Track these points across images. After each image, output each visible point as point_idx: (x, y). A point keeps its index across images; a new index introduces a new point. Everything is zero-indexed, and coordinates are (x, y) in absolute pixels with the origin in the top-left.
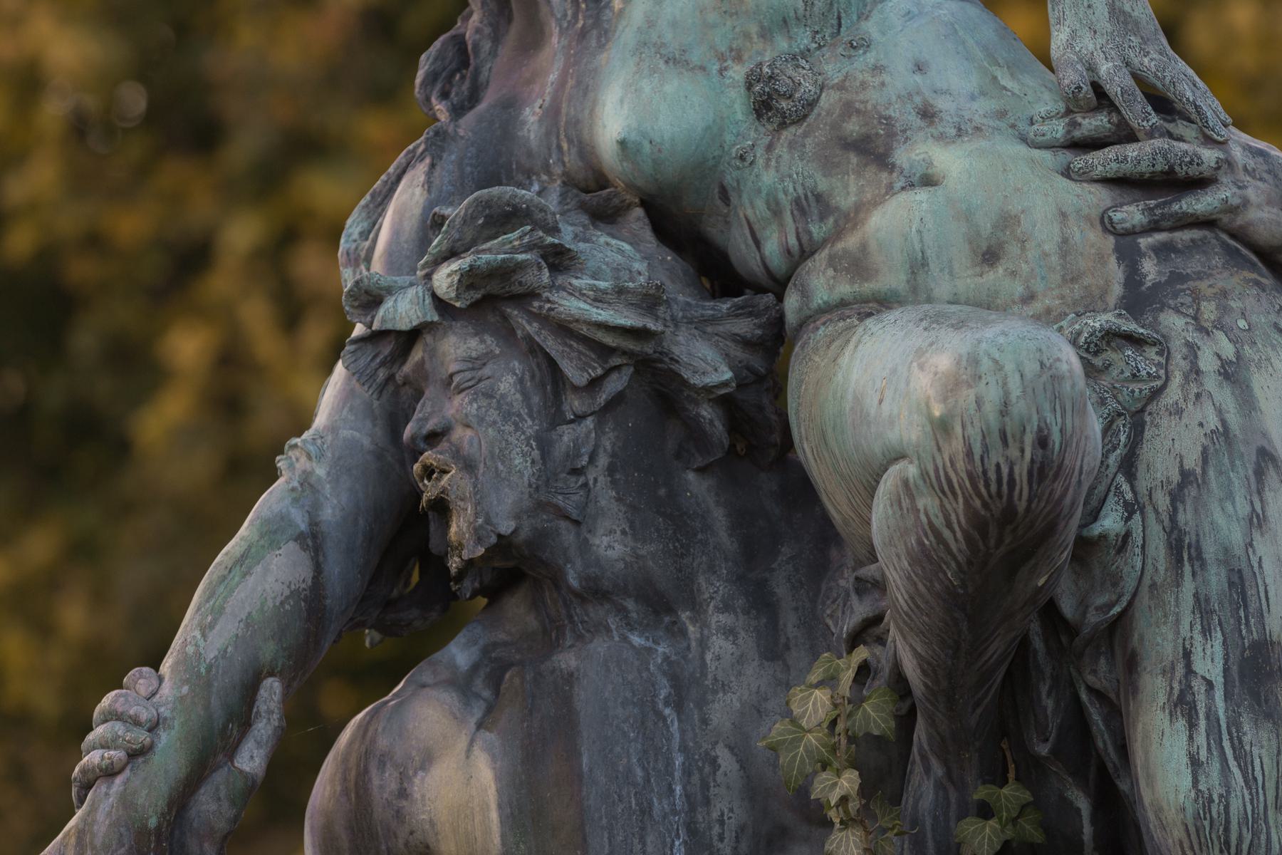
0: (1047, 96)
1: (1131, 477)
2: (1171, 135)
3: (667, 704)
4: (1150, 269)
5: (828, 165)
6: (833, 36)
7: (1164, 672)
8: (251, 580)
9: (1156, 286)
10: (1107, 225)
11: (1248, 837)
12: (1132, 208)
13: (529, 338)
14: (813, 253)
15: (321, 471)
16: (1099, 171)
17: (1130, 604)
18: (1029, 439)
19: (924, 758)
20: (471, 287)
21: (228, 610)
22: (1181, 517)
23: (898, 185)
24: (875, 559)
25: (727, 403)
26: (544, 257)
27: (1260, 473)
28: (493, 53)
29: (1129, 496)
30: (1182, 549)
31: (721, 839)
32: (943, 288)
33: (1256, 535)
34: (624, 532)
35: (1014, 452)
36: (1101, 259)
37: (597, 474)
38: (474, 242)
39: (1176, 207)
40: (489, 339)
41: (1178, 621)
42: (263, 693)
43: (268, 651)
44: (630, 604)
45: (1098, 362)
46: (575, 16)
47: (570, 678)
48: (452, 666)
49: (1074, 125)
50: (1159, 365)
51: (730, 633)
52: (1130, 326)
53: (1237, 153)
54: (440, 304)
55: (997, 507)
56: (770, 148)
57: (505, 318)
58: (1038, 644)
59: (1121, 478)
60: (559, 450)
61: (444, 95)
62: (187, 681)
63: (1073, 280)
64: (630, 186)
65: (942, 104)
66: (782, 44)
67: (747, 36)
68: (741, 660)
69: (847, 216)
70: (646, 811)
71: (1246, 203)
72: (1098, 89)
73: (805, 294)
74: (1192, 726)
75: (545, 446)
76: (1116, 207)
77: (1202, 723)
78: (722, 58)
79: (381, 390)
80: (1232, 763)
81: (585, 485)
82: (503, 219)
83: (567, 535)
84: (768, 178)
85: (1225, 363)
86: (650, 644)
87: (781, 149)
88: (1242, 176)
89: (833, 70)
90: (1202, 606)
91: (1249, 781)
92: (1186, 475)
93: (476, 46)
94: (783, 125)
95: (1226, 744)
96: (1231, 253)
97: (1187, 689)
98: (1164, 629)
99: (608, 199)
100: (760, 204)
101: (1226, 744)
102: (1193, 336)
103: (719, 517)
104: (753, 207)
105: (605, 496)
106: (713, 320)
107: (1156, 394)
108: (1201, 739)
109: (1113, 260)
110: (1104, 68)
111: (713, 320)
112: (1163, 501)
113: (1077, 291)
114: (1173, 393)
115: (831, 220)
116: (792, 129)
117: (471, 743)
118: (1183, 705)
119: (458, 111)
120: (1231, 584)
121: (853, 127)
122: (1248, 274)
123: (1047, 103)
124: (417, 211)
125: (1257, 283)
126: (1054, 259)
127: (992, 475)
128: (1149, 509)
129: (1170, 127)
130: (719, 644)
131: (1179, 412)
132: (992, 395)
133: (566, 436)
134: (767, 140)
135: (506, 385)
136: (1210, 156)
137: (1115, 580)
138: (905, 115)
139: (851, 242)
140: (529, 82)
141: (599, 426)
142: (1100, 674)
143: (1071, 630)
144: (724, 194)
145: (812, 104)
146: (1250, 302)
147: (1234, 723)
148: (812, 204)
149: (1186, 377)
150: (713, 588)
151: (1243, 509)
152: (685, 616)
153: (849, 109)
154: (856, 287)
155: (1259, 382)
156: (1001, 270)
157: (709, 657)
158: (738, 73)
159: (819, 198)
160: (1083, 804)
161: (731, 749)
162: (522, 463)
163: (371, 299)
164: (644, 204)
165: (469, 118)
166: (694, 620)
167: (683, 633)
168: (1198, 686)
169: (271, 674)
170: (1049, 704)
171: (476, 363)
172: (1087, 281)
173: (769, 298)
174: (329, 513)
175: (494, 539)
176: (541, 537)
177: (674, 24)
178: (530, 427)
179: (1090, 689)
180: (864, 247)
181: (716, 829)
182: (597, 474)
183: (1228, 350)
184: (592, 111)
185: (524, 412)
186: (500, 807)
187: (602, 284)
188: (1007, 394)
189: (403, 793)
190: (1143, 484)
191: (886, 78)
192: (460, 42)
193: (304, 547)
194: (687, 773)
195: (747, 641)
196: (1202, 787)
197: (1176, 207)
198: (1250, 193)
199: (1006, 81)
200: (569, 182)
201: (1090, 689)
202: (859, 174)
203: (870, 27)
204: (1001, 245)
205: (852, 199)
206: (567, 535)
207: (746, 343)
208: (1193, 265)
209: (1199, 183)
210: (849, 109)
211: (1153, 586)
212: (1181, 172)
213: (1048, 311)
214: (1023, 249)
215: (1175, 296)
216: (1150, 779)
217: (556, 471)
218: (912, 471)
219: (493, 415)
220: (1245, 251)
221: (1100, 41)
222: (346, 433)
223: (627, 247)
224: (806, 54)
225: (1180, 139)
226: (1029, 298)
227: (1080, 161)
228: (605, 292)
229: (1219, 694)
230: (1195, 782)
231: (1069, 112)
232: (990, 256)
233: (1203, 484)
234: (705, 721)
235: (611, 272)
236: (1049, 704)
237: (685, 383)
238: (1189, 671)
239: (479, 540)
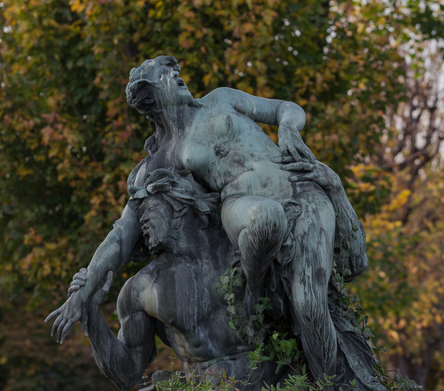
0: (277, 152)
2: (303, 161)
3: (194, 278)
4: (298, 189)
6: (233, 138)
7: (299, 274)
8: (107, 250)
9: (300, 193)
10: (290, 180)
11: (316, 310)
12: (295, 176)
13: (167, 201)
14: (227, 184)
15: (122, 227)
16: (288, 168)
17: (292, 260)
18: (272, 225)
19: (248, 291)
20: (155, 189)
21: (102, 256)
22: (304, 242)
23: (246, 170)
24: (239, 249)
25: (208, 215)
26: (171, 184)
27: (320, 233)
28: (161, 140)
29: (293, 237)
30: (303, 248)
31: (205, 307)
32: (254, 192)
33: (319, 246)
34: (186, 242)
35: (269, 227)
36: (288, 187)
37: (181, 230)
38: (156, 180)
39: (304, 176)
40: (158, 200)
41: (302, 264)
42: (109, 274)
43: (110, 265)
44: (187, 257)
45: (287, 208)
46: (178, 133)
47: (174, 272)
48: (149, 270)
49: (283, 158)
50: (300, 210)
51: (208, 264)
52: (294, 201)
53: (317, 165)
54: (148, 193)
55: (265, 239)
56: (219, 162)
57: (162, 196)
58: (273, 268)
59: (291, 233)
60: (173, 224)
61: (150, 149)
62: (93, 271)
63: (282, 191)
64: (189, 169)
65: (255, 153)
66: (222, 140)
67: (215, 138)
68: (210, 270)
69: (235, 177)
70: (189, 301)
71: (319, 176)
72: (288, 151)
73: (225, 193)
74: (305, 286)
75: (170, 223)
76: (292, 176)
77: (307, 285)
78: (209, 143)
79: (135, 211)
80: (313, 294)
81: (178, 232)
82: (163, 175)
83: (174, 242)
84: (218, 168)
85: (313, 210)
86: (191, 266)
87: (221, 162)
88: (318, 170)
89: (232, 145)
90: (308, 261)
91: (317, 298)
92: (305, 233)
93: (157, 139)
94: (222, 157)
95: (312, 290)
96: (315, 186)
98: (299, 265)
99: (184, 172)
100: (216, 174)
101: (312, 290)
102: (307, 204)
103: (206, 239)
104: (215, 174)
105: (182, 234)
106: (206, 198)
107: (299, 216)
108: (307, 289)
109: (291, 187)
110: (290, 147)
111: (206, 198)
112: (300, 238)
113: (283, 194)
114: (303, 216)
115: (231, 177)
116: (224, 158)
117: (153, 286)
118: (303, 281)
119: (153, 152)
120: (314, 256)
121: (236, 158)
122: (319, 191)
123: (278, 154)
124: (144, 173)
125: (321, 193)
126: (278, 187)
127: (264, 232)
128: (297, 240)
129: (303, 159)
130: (205, 266)
131: (304, 220)
132: (264, 215)
133: (174, 221)
134: (218, 160)
135: (162, 210)
136: (311, 166)
137: (289, 255)
138: (247, 156)
139: (235, 182)
140: (168, 147)
141: (181, 220)
142: (286, 274)
143: (280, 265)
144: (209, 171)
145: (228, 153)
146: (319, 197)
147: (314, 286)
148: (227, 174)
149: (305, 212)
150: (205, 254)
152: (198, 260)
153: (236, 154)
154: (236, 192)
155: (321, 214)
156: (267, 189)
157: (203, 269)
158: (213, 146)
159: (229, 172)
160: (281, 302)
161: (207, 288)
162: (165, 227)
163: (134, 191)
164: (192, 173)
165: (155, 154)
166: (200, 261)
167: (198, 264)
168: (306, 277)
169: (111, 270)
170: (275, 280)
171: (156, 205)
172: (285, 191)
173: (218, 193)
174: (124, 236)
175: (158, 243)
176: (168, 242)
177: (199, 135)
178: (167, 219)
179: (284, 278)
180: (238, 183)
181: (204, 305)
182: (181, 230)
183: (314, 207)
184: (181, 153)
185: (166, 216)
186: (158, 299)
187: (183, 190)
188: (267, 215)
189: (138, 296)
190: (296, 234)
191: (243, 147)
192: (154, 138)
193: (118, 244)
194: (198, 293)
195: (211, 266)
196: (307, 299)
197: (304, 176)
198: (320, 174)
199: (269, 149)
200: (176, 168)
201: (284, 278)
202: (237, 168)
203: (241, 137)
204: (267, 183)
205: (236, 173)
206: (174, 242)
207: (213, 203)
208: (308, 188)
209: (309, 171)
210: (236, 154)
211: (297, 256)
212: (305, 169)
213: (277, 198)
214: (272, 184)
215: (304, 195)
216: (296, 298)
217: (172, 229)
219: (159, 217)
220: (318, 186)
221: (289, 141)
222: (128, 220)
223: (188, 182)
224: (227, 142)
225: (305, 162)
226: (273, 195)
227: (284, 166)
228: (183, 191)
229: (311, 279)
230: (305, 298)
231: (282, 156)
232: (265, 186)
233: (308, 235)
234: (202, 282)
235: (184, 187)
236: (275, 280)
237: (199, 211)
238: (305, 274)
239: (155, 243)
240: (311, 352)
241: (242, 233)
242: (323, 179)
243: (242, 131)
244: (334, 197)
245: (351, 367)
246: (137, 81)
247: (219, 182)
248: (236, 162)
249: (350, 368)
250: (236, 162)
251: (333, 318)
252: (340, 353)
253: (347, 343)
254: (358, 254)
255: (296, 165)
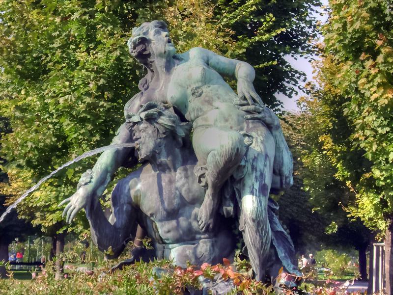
1: (246, 157)
5: (203, 104)
18: (236, 149)
19: (208, 195)
25: (183, 139)
27: (266, 158)
28: (151, 82)
30: (254, 168)
37: (163, 147)
43: (109, 169)
54: (141, 119)
56: (194, 100)
58: (229, 181)
67: (192, 83)
68: (181, 178)
73: (197, 123)
78: (187, 86)
91: (261, 206)
92: (255, 157)
97: (253, 190)
102: (257, 136)
112: (251, 161)
121: (207, 99)
135: (150, 132)
136: (261, 109)
137: (243, 172)
139: (205, 116)
151: (264, 163)
153: (206, 96)
159: (201, 109)
168: (255, 190)
171: (146, 128)
179: (237, 189)
182: (163, 147)
201: (237, 189)
207: (187, 129)
218: (216, 152)
226: (231, 128)
227: (241, 108)
229: (258, 191)
232: (226, 120)
240: (252, 244)
241: (210, 155)
242: (268, 120)
243: (212, 80)
244: (274, 132)
245: (280, 257)
246: (138, 37)
247: (192, 116)
248: (206, 101)
249: (279, 258)
250: (206, 101)
251: (269, 220)
252: (272, 246)
253: (277, 239)
254: (287, 175)
255: (251, 107)
